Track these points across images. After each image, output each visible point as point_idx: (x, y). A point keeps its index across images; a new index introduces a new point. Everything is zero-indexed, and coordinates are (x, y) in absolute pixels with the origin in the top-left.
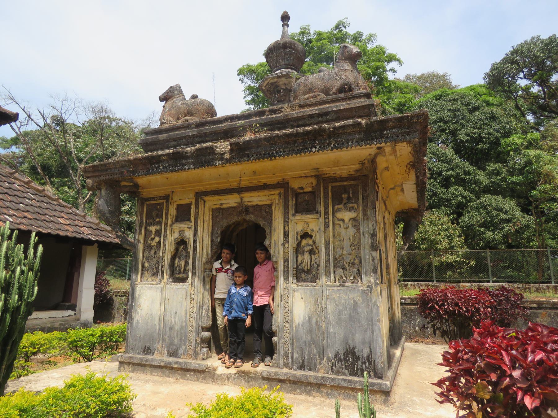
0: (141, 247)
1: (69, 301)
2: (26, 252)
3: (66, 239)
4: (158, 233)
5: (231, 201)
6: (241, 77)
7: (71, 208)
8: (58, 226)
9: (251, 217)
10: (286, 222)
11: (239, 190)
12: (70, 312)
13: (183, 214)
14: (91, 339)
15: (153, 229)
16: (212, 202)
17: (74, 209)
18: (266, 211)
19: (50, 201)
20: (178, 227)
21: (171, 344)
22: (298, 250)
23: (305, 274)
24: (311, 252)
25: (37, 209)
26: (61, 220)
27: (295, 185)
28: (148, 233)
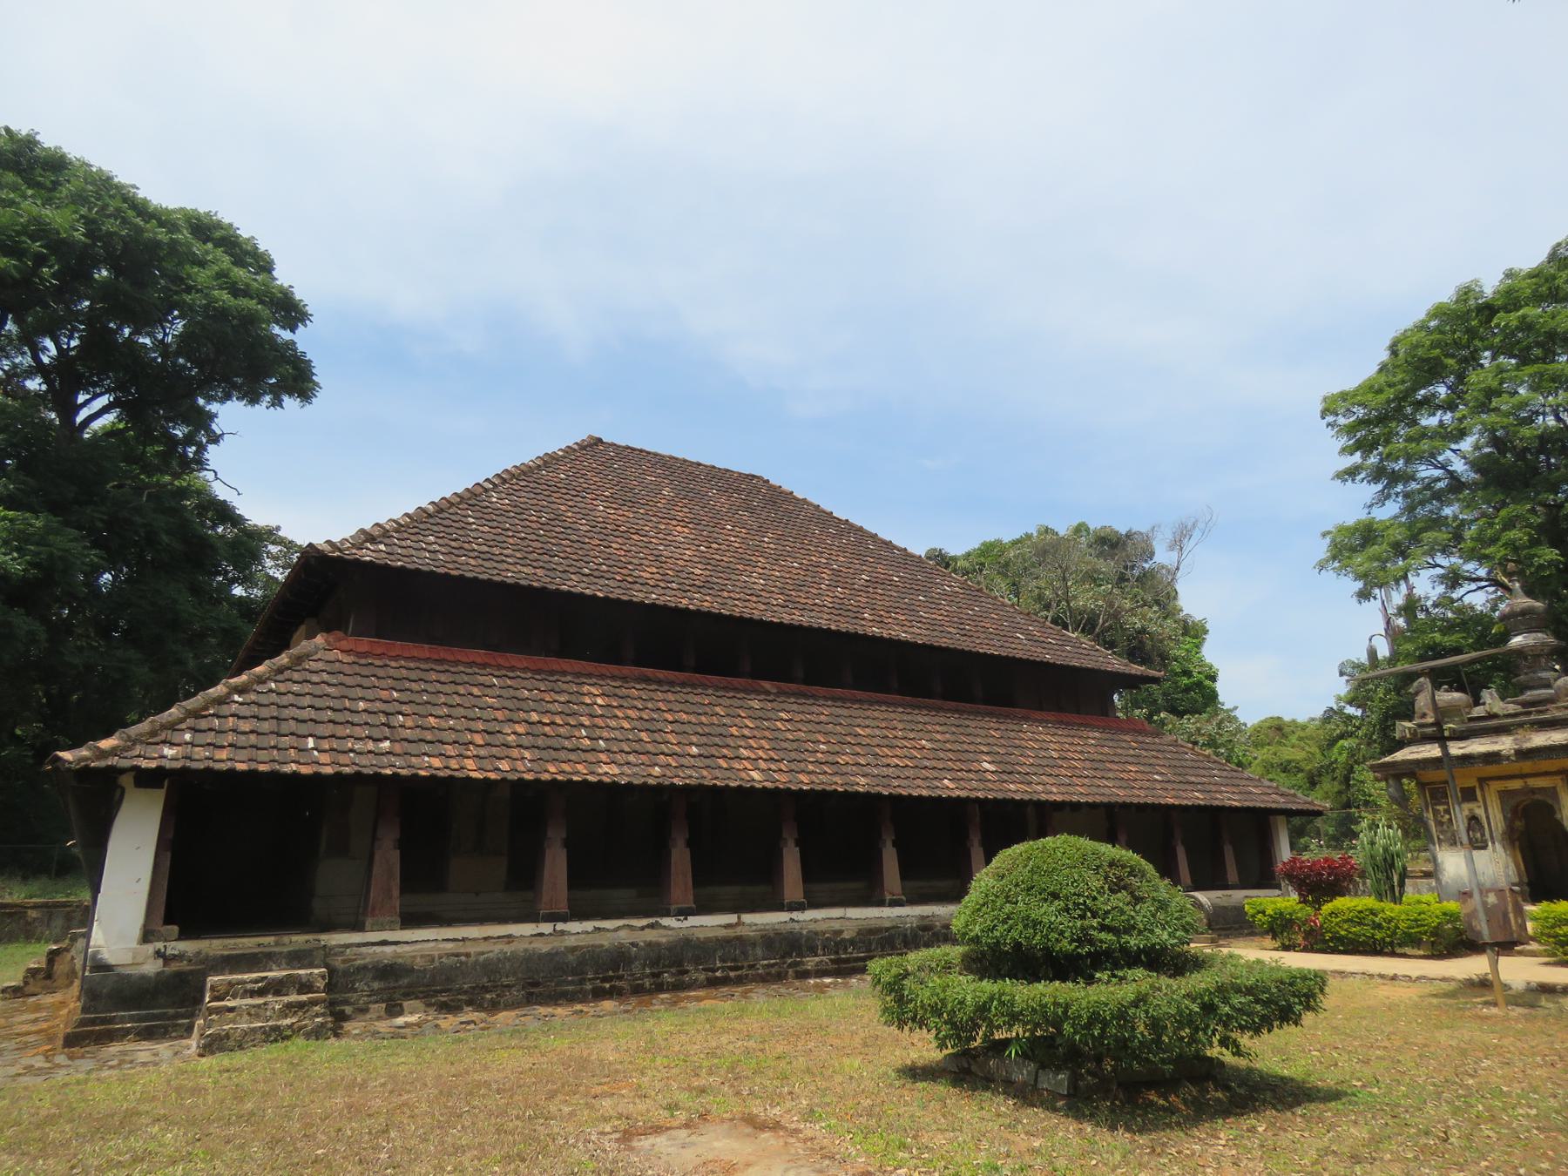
0: (1432, 823)
4: (1447, 811)
5: (1516, 784)
6: (1330, 419)
9: (1538, 797)
11: (1522, 776)
13: (1469, 795)
15: (1441, 808)
16: (1496, 786)
18: (1553, 792)
20: (1466, 806)
28: (1436, 812)
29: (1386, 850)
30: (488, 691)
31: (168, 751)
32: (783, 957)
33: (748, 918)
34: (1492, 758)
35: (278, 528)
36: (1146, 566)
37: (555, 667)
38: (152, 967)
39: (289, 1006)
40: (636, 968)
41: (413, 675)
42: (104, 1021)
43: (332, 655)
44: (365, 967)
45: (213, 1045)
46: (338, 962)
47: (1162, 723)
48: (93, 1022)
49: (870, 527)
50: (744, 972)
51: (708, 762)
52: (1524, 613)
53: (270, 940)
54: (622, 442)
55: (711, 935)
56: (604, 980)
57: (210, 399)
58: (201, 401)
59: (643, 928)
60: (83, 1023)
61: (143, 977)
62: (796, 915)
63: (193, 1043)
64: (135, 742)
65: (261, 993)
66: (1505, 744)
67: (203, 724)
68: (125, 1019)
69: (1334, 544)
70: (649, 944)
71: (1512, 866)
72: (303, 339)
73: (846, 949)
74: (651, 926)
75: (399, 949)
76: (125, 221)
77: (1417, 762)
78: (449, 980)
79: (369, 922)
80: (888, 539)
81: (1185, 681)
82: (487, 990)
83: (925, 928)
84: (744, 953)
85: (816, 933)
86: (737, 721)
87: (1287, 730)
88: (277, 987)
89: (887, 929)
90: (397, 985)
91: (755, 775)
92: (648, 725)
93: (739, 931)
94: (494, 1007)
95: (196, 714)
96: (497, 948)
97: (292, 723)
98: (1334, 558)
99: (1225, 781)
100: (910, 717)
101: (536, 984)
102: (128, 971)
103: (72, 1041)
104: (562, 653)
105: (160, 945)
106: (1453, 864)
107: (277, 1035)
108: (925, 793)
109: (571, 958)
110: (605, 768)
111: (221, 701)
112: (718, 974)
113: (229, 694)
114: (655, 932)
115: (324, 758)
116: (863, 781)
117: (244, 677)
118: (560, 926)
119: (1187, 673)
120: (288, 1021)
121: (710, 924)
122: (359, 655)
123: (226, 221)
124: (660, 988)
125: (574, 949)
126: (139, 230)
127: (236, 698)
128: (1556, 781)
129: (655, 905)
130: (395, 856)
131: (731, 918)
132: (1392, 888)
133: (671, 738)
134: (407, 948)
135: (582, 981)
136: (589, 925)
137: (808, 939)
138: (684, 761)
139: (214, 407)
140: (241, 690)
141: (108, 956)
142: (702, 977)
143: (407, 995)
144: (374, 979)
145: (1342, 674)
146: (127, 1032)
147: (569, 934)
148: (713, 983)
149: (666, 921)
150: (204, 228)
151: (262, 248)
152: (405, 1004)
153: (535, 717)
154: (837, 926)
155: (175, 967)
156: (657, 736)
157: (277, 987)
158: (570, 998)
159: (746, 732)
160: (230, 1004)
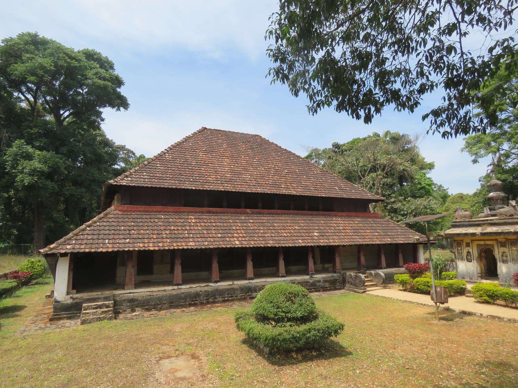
4: (461, 250)
5: (482, 243)
10: (498, 249)
11: (484, 240)
13: (468, 245)
15: (459, 248)
16: (476, 243)
18: (493, 246)
20: (467, 248)
21: (470, 277)
22: (502, 256)
23: (504, 262)
24: (506, 256)
27: (500, 240)
28: (458, 250)
29: (436, 263)
30: (160, 220)
31: (68, 247)
32: (246, 293)
33: (236, 282)
34: (473, 234)
35: (125, 146)
36: (409, 146)
37: (182, 210)
38: (70, 301)
39: (103, 312)
40: (202, 298)
41: (139, 217)
42: (59, 315)
43: (116, 212)
44: (125, 300)
45: (83, 323)
46: (118, 299)
47: (409, 201)
48: (56, 315)
49: (293, 151)
51: (223, 239)
52: (494, 185)
53: (100, 293)
54: (213, 128)
56: (192, 301)
60: (54, 315)
61: (68, 304)
62: (251, 281)
63: (79, 321)
64: (60, 245)
65: (96, 308)
66: (478, 230)
67: (78, 237)
68: (64, 314)
69: (467, 142)
70: (206, 291)
71: (479, 268)
72: (123, 91)
74: (207, 286)
75: (134, 294)
76: (65, 61)
77: (452, 234)
78: (148, 302)
79: (126, 288)
80: (298, 155)
81: (419, 186)
82: (159, 305)
84: (234, 293)
86: (236, 224)
87: (464, 197)
88: (100, 307)
90: (134, 304)
91: (237, 243)
92: (207, 228)
93: (233, 286)
94: (161, 309)
95: (77, 235)
97: (102, 235)
98: (467, 147)
99: (402, 234)
100: (294, 218)
101: (173, 303)
103: (51, 320)
104: (186, 205)
105: (71, 295)
106: (462, 266)
107: (99, 319)
108: (291, 245)
109: (182, 295)
110: (191, 244)
111: (84, 230)
112: (226, 299)
113: (86, 228)
115: (110, 246)
116: (271, 242)
117: (90, 222)
118: (179, 287)
119: (420, 184)
120: (103, 316)
121: (224, 284)
122: (124, 211)
123: (98, 52)
124: (208, 303)
125: (183, 293)
126: (69, 63)
127: (88, 229)
128: (494, 243)
129: (208, 280)
131: (231, 283)
132: (437, 274)
133: (213, 232)
135: (186, 302)
136: (188, 286)
138: (216, 239)
139: (101, 110)
140: (89, 226)
141: (58, 299)
142: (221, 299)
143: (137, 307)
144: (128, 302)
145: (480, 181)
146: (64, 317)
148: (224, 301)
149: (211, 284)
150: (90, 56)
151: (110, 60)
152: (136, 309)
153: (172, 228)
155: (76, 301)
156: (209, 232)
157: (100, 307)
158: (183, 306)
159: (238, 228)
160: (87, 311)
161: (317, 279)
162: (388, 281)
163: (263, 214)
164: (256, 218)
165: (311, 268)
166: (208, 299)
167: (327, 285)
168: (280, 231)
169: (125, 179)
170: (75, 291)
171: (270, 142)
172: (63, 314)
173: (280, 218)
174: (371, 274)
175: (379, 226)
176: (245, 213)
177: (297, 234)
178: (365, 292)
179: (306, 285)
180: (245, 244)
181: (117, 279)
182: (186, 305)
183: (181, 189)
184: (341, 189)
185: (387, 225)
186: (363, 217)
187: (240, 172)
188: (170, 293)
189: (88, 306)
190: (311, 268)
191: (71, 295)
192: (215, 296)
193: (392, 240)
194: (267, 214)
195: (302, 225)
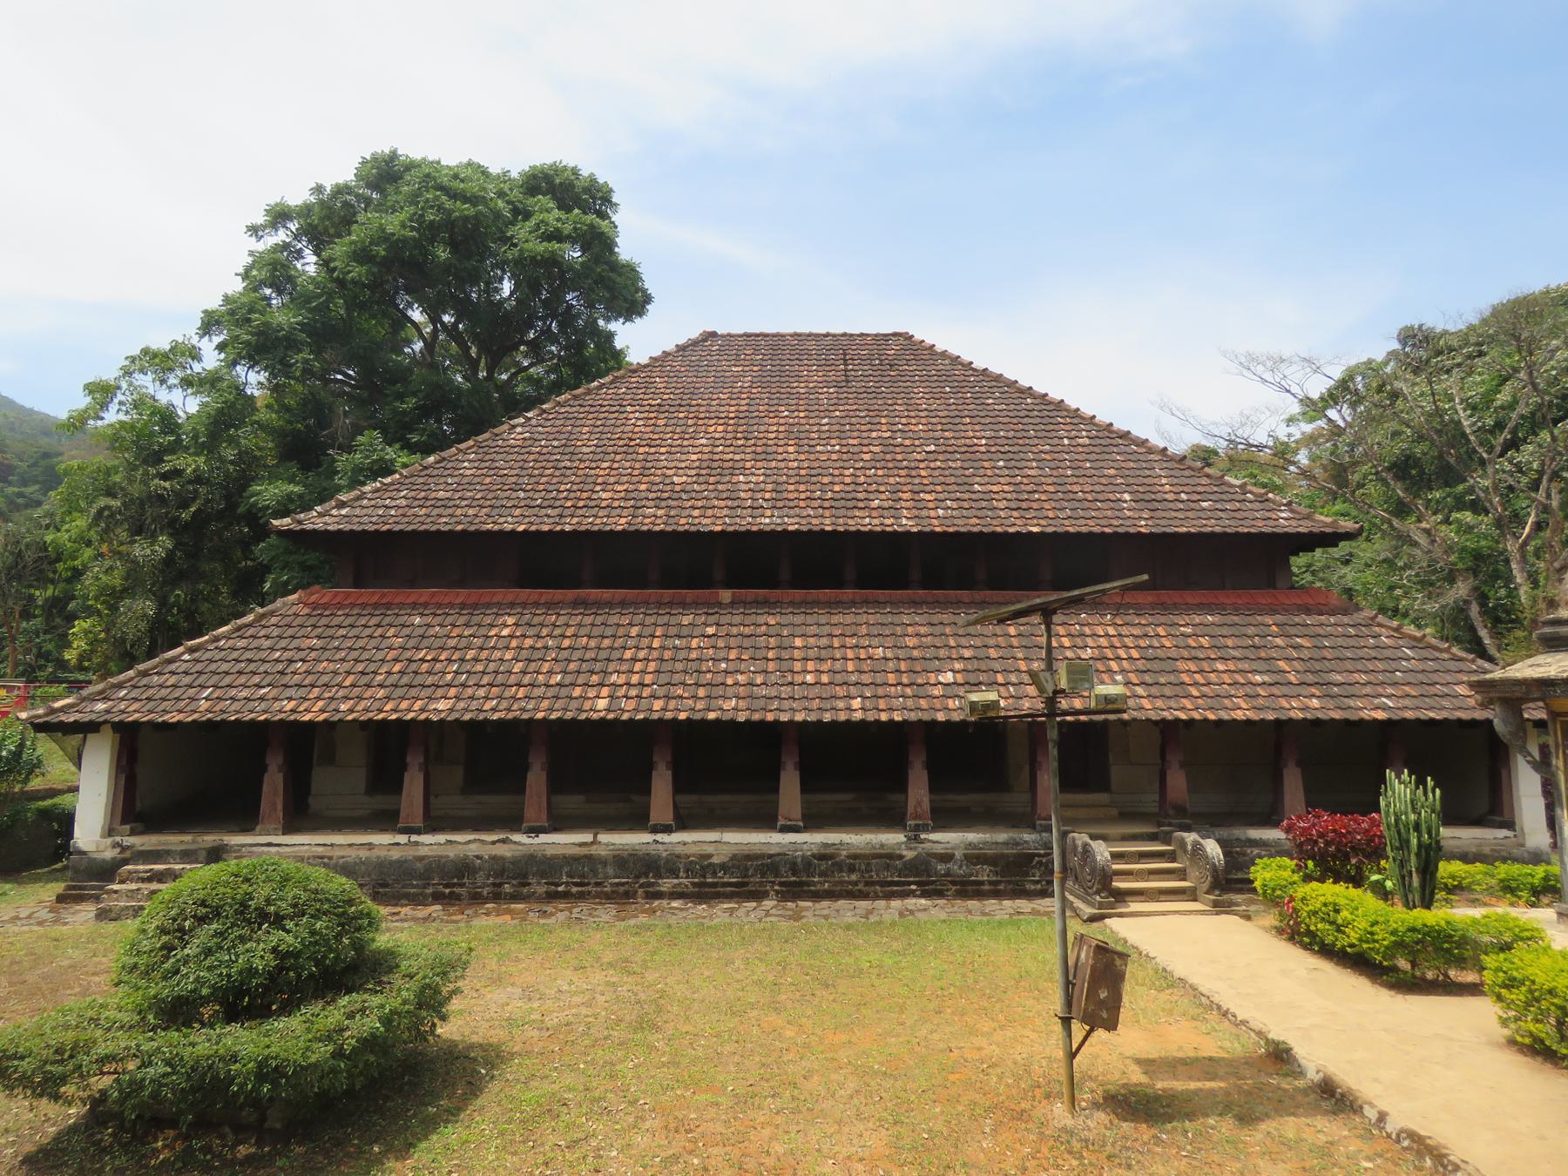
1: (1501, 814)
2: (1425, 793)
3: (1473, 723)
7: (1473, 661)
8: (1457, 702)
12: (1503, 833)
14: (1530, 879)
17: (1480, 662)
19: (1437, 654)
25: (1420, 677)
26: (1461, 690)
31: (101, 706)
32: (638, 877)
33: (604, 838)
37: (495, 600)
38: (109, 854)
40: (480, 879)
42: (81, 888)
45: (102, 915)
48: (74, 888)
50: (590, 888)
53: (188, 838)
55: (560, 851)
56: (446, 886)
57: (608, 320)
58: (601, 322)
59: (494, 843)
62: (659, 837)
64: (83, 700)
65: (149, 880)
67: (145, 681)
70: (493, 858)
73: (714, 874)
74: (503, 841)
75: (280, 849)
76: (440, 208)
83: (822, 857)
84: (595, 872)
85: (678, 856)
89: (770, 856)
93: (594, 850)
95: (145, 674)
96: (353, 854)
99: (1410, 678)
101: (385, 885)
102: (95, 856)
105: (118, 839)
114: (506, 846)
118: (414, 838)
124: (497, 897)
127: (187, 657)
129: (513, 822)
130: (279, 779)
131: (587, 837)
134: (287, 849)
136: (441, 838)
137: (667, 861)
140: (192, 650)
142: (541, 890)
147: (423, 844)
148: (552, 896)
149: (517, 837)
151: (601, 181)
154: (710, 849)
161: (939, 849)
162: (1229, 885)
163: (777, 603)
164: (737, 619)
165: (919, 803)
166: (500, 885)
167: (984, 874)
168: (798, 666)
169: (334, 512)
170: (128, 827)
171: (936, 354)
172: (93, 888)
173: (835, 619)
174: (1183, 844)
175: (1297, 647)
176: (708, 604)
177: (866, 679)
178: (1101, 917)
179: (887, 867)
180: (628, 710)
181: (311, 800)
182: (425, 896)
183: (478, 533)
184: (1148, 499)
185: (1352, 642)
186: (1237, 610)
187: (740, 464)
188: (382, 853)
189: (130, 872)
190: (919, 803)
191: (118, 839)
192: (525, 876)
193: (1330, 703)
194: (792, 604)
195: (911, 642)
